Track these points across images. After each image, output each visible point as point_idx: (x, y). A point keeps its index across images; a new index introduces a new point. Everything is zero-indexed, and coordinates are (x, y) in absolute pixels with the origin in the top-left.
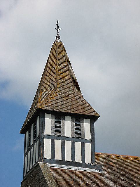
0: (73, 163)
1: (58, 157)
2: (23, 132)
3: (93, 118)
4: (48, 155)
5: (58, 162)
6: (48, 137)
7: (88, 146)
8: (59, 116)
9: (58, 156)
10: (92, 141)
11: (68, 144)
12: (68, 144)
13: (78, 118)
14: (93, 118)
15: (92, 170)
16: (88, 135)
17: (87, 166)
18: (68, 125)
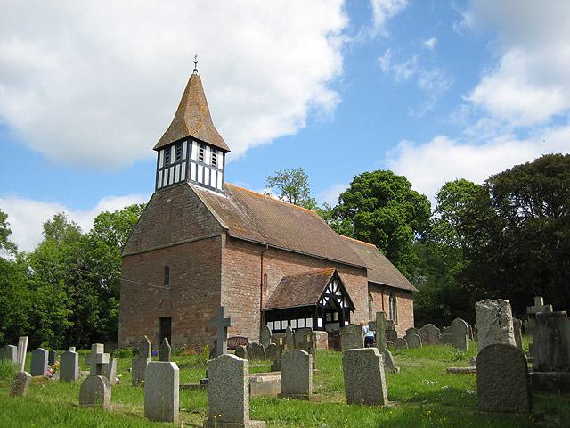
0: (209, 187)
1: (200, 180)
2: (158, 149)
3: (225, 151)
4: (193, 177)
5: (200, 184)
6: (194, 161)
7: (220, 174)
8: (202, 144)
9: (200, 180)
10: (223, 171)
11: (207, 170)
12: (207, 170)
13: (215, 149)
14: (225, 151)
15: (222, 196)
16: (220, 167)
17: (218, 191)
18: (208, 152)
